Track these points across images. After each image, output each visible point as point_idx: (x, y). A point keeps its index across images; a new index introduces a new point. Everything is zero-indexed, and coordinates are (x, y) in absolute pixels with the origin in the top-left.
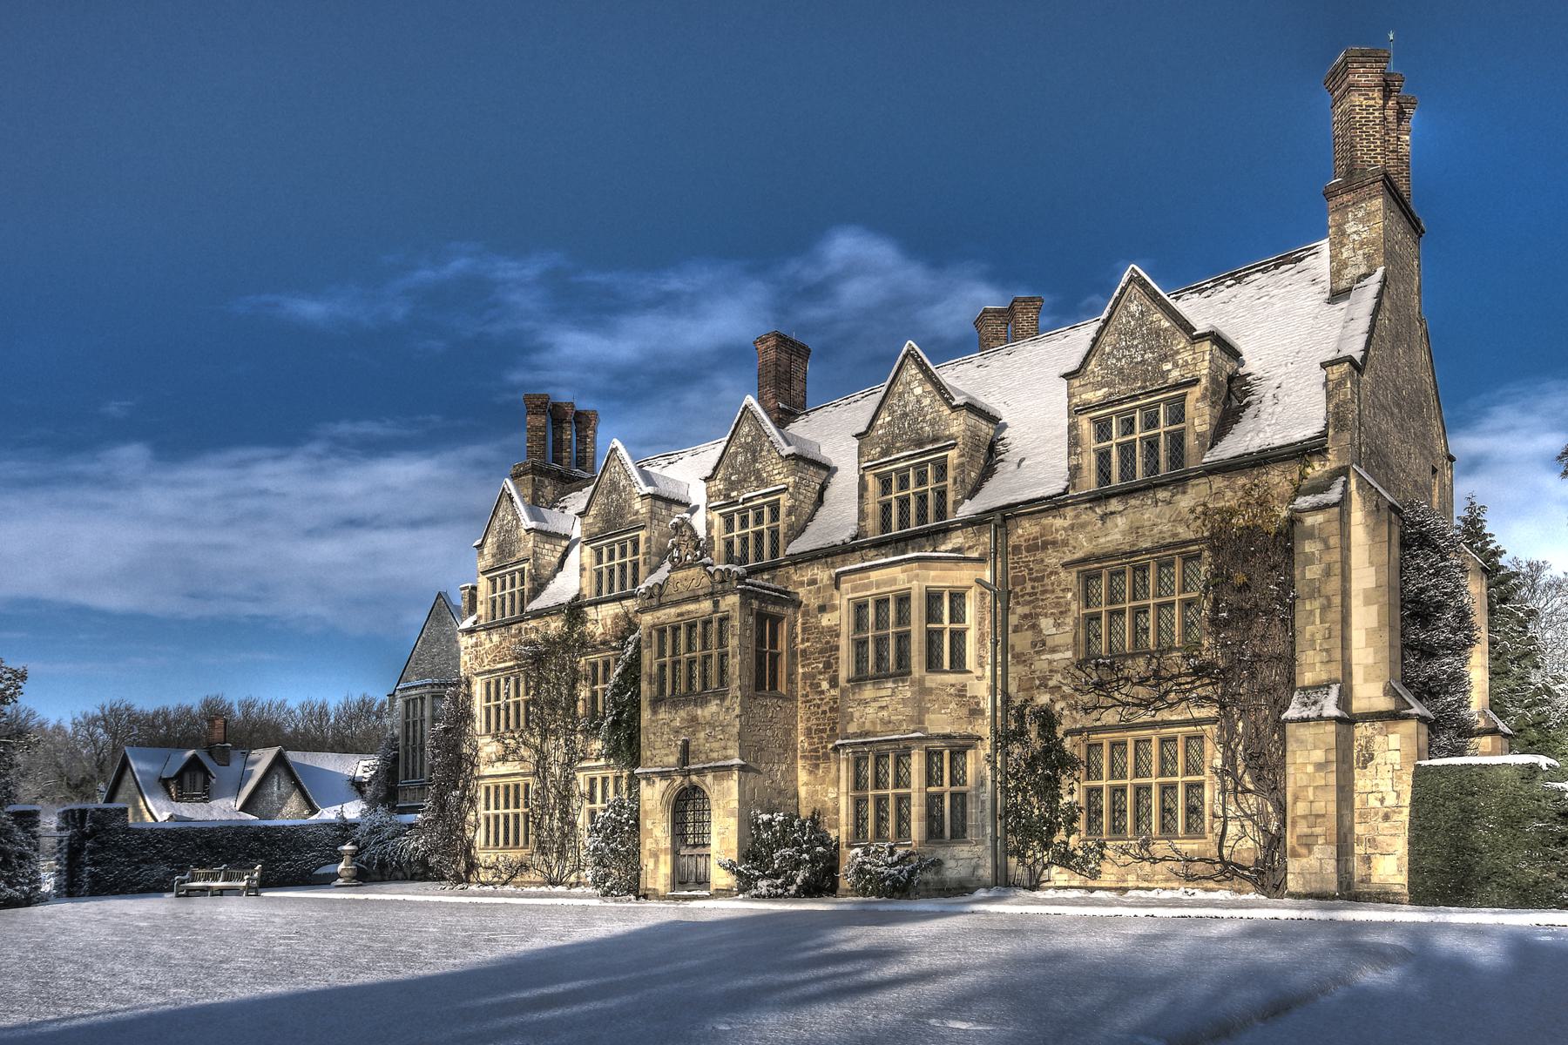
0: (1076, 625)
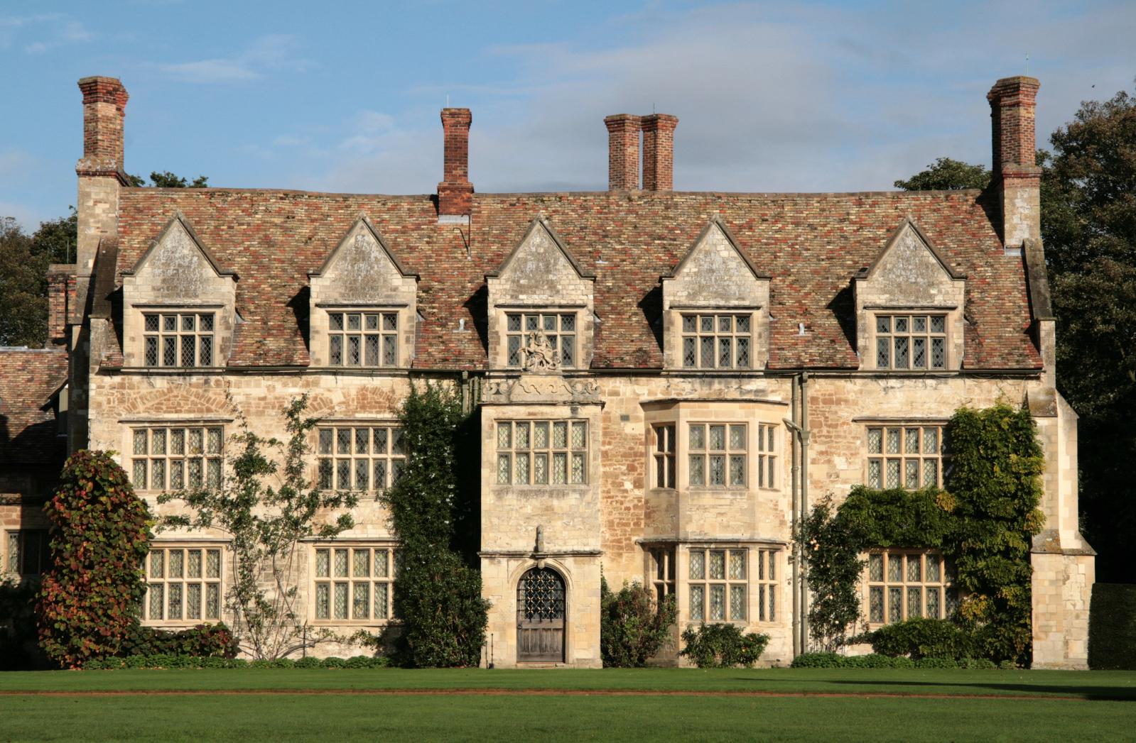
0: (863, 465)
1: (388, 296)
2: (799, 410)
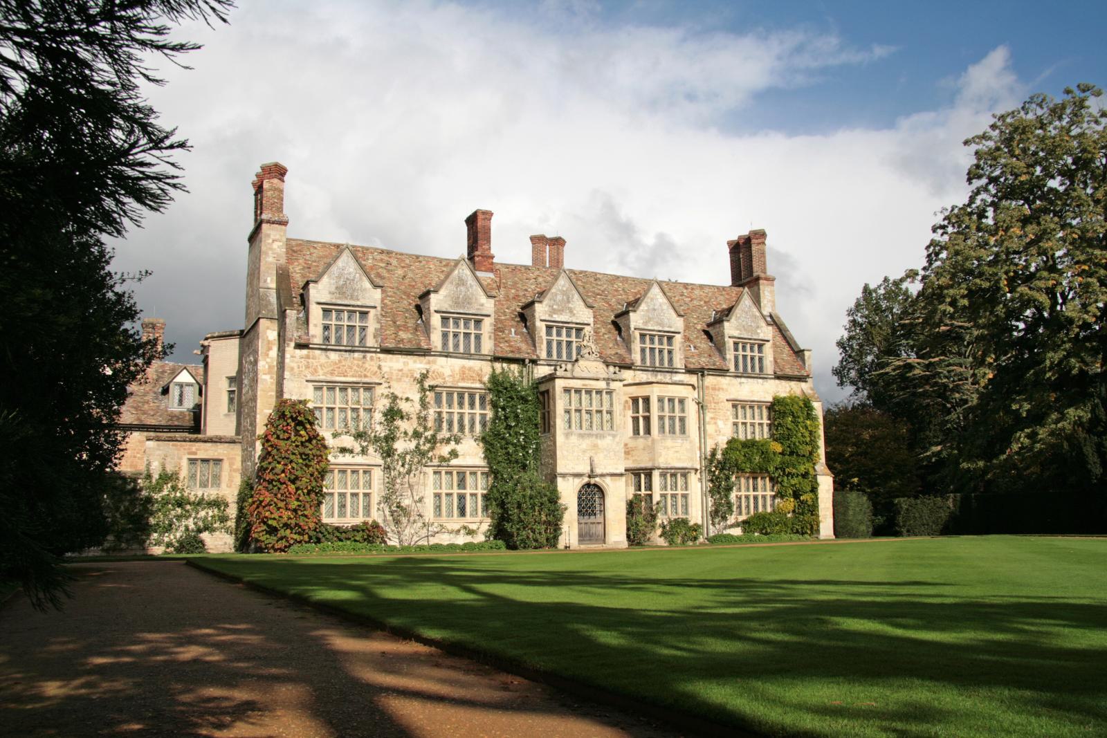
1: (479, 309)
2: (701, 393)
